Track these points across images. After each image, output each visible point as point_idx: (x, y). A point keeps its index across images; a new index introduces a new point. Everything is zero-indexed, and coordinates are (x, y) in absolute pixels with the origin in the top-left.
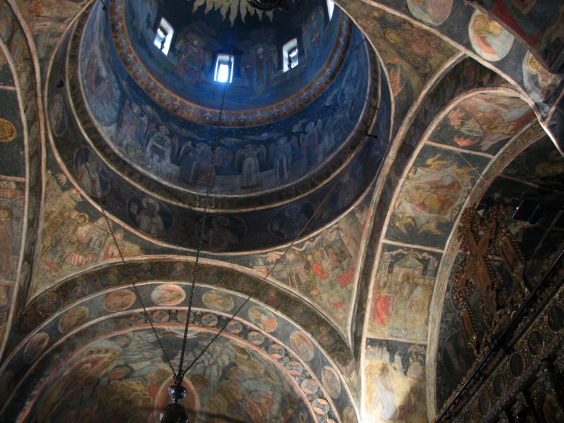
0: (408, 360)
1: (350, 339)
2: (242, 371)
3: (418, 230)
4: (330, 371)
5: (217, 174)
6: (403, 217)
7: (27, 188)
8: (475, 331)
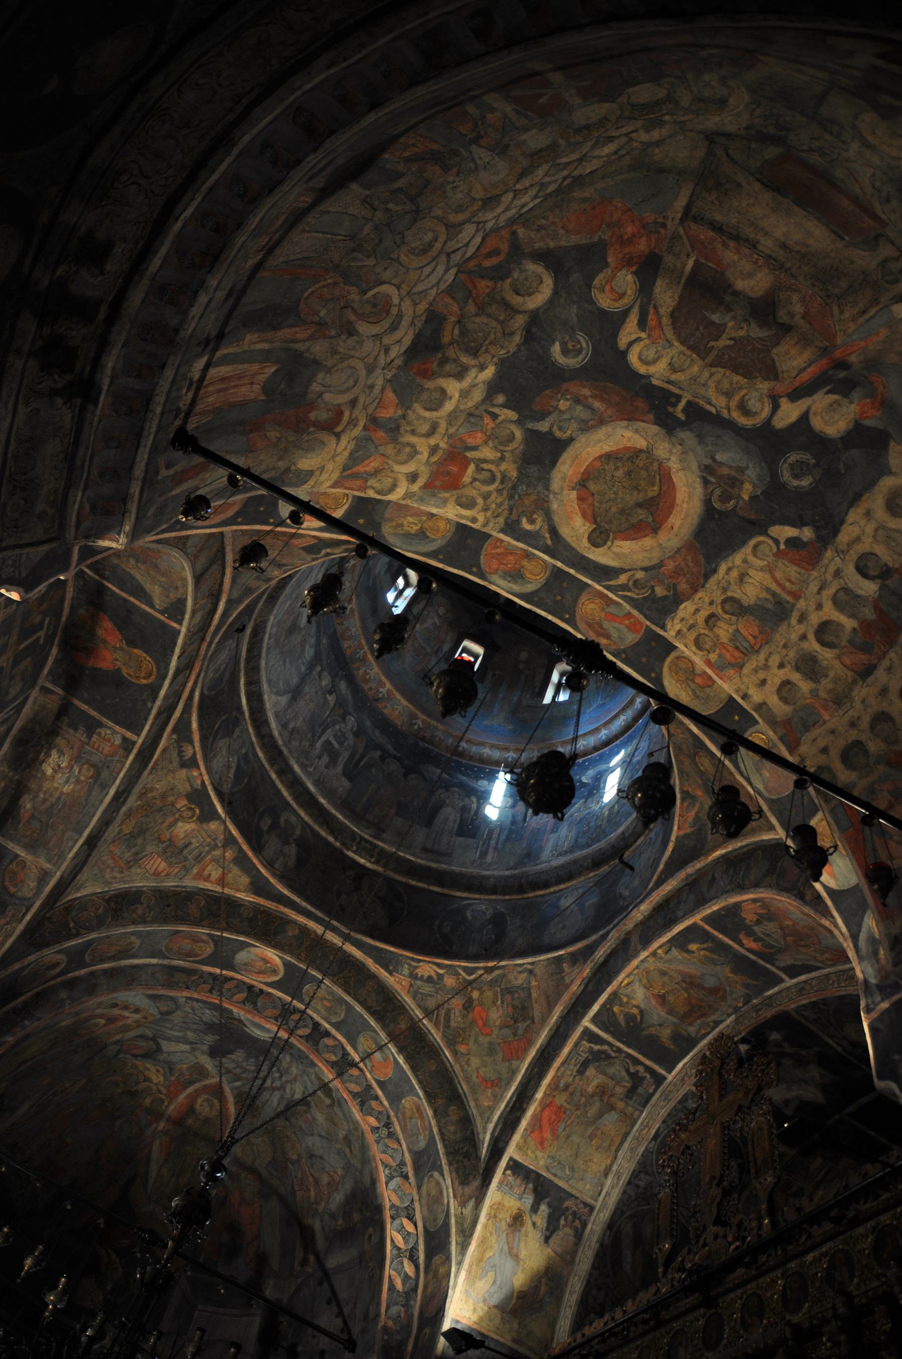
0: (558, 1220)
1: (486, 1145)
2: (314, 1119)
3: (644, 1029)
4: (438, 1183)
5: (397, 814)
6: (627, 1003)
7: (135, 751)
8: (672, 1236)
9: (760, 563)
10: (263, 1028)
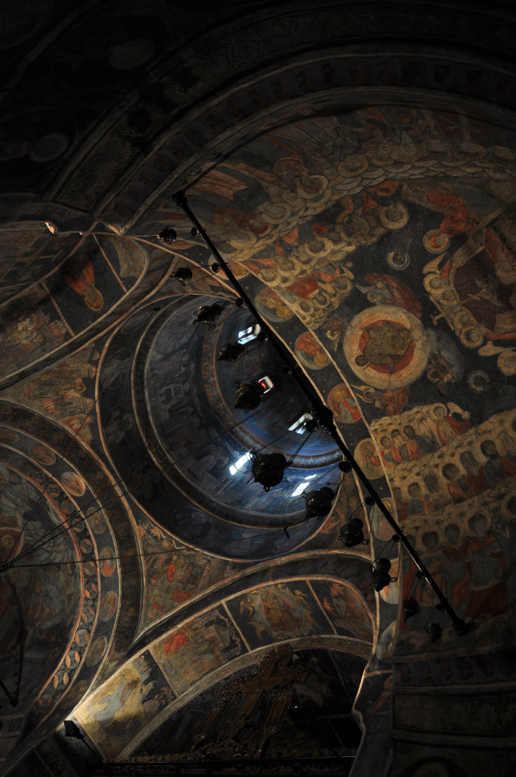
4: (104, 644)
9: (435, 417)
10: (58, 517)
